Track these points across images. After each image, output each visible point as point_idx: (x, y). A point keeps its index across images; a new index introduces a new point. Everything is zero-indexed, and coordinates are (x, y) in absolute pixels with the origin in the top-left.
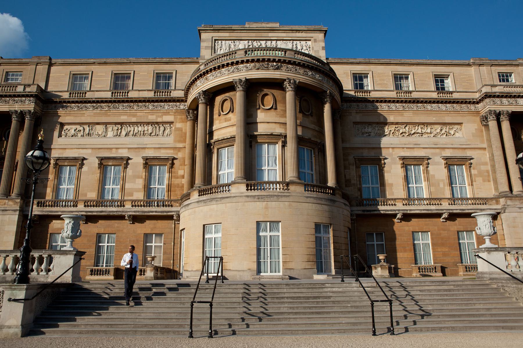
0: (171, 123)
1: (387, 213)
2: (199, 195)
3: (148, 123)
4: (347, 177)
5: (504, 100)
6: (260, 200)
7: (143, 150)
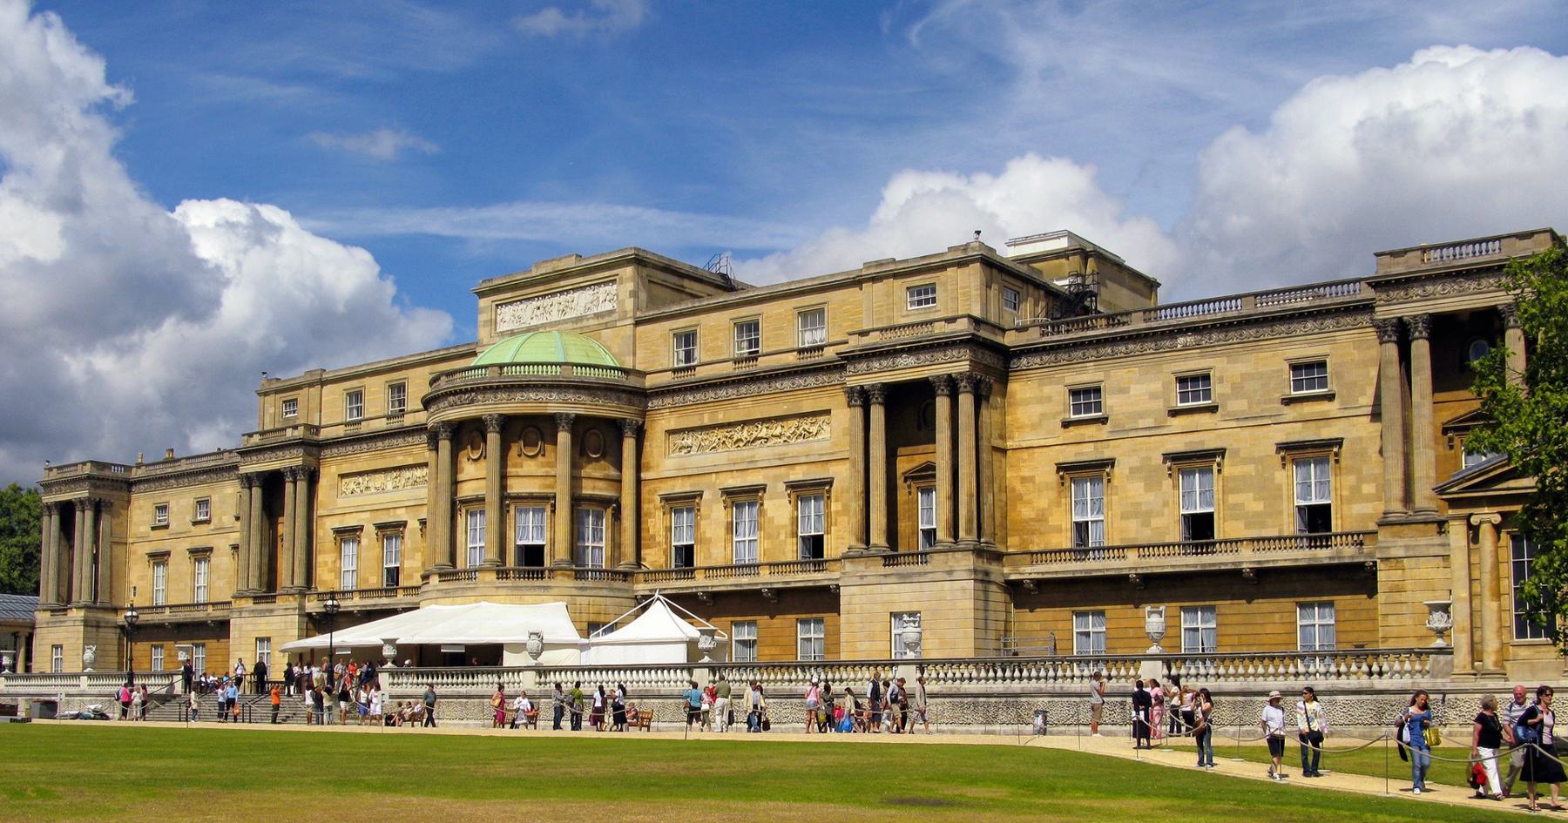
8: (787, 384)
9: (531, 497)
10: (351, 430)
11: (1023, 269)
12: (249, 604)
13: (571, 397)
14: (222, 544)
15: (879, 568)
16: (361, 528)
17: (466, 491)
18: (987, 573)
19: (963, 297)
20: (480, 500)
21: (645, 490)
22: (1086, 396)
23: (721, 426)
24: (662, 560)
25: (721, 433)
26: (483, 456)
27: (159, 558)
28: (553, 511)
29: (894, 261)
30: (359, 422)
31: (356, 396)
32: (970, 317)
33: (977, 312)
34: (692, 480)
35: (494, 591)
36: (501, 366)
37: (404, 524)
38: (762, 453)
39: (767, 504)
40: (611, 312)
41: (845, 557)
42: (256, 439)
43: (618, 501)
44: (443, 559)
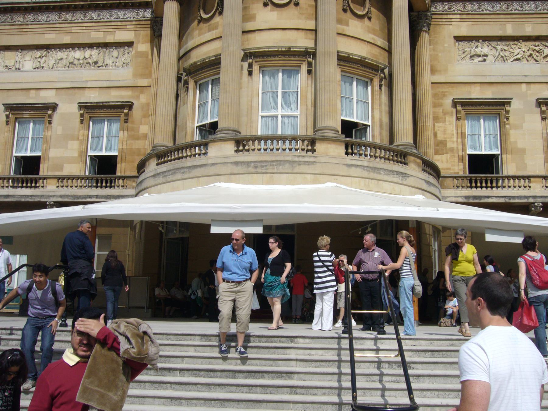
0: (130, 44)
1: (512, 201)
2: (158, 164)
3: (91, 46)
4: (440, 137)
6: (259, 170)
7: (81, 91)
34: (494, 88)
35: (344, 170)
37: (54, 107)
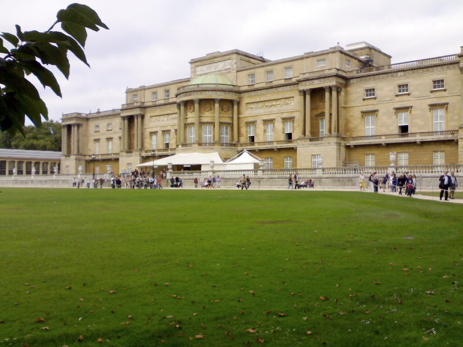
5: (307, 82)
8: (281, 88)
9: (208, 123)
10: (154, 103)
11: (351, 54)
12: (124, 154)
13: (219, 93)
14: (116, 137)
15: (309, 142)
16: (157, 132)
17: (189, 121)
18: (340, 143)
19: (334, 64)
20: (193, 124)
21: (241, 120)
22: (370, 92)
23: (262, 101)
24: (245, 140)
25: (262, 104)
26: (194, 111)
27: (97, 140)
28: (214, 127)
29: (313, 52)
30: (156, 101)
31: (155, 93)
32: (336, 68)
33: (338, 67)
36: (198, 85)
37: (170, 130)
38: (274, 109)
39: (276, 124)
40: (229, 69)
41: (299, 139)
42: (125, 106)
43: (233, 124)
44: (182, 140)
